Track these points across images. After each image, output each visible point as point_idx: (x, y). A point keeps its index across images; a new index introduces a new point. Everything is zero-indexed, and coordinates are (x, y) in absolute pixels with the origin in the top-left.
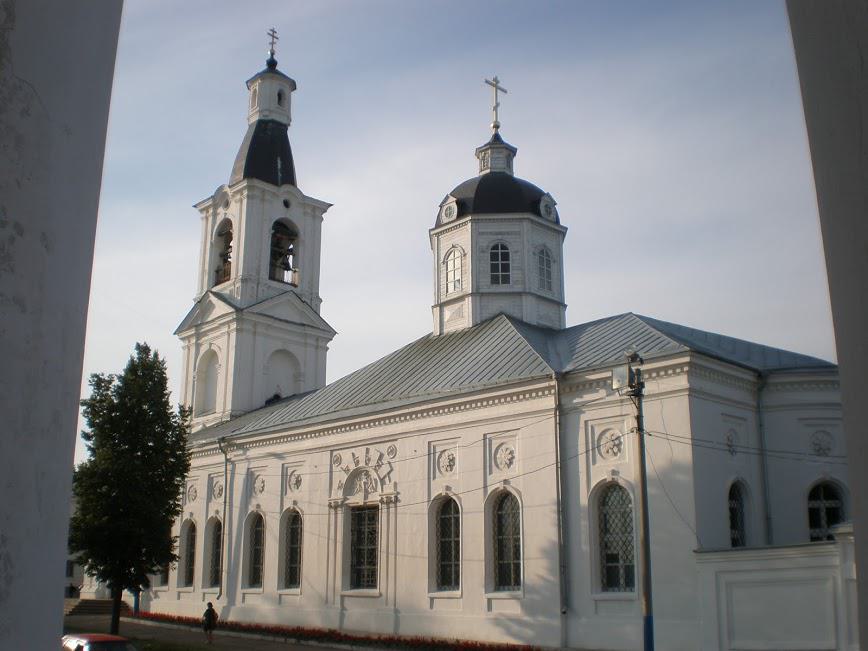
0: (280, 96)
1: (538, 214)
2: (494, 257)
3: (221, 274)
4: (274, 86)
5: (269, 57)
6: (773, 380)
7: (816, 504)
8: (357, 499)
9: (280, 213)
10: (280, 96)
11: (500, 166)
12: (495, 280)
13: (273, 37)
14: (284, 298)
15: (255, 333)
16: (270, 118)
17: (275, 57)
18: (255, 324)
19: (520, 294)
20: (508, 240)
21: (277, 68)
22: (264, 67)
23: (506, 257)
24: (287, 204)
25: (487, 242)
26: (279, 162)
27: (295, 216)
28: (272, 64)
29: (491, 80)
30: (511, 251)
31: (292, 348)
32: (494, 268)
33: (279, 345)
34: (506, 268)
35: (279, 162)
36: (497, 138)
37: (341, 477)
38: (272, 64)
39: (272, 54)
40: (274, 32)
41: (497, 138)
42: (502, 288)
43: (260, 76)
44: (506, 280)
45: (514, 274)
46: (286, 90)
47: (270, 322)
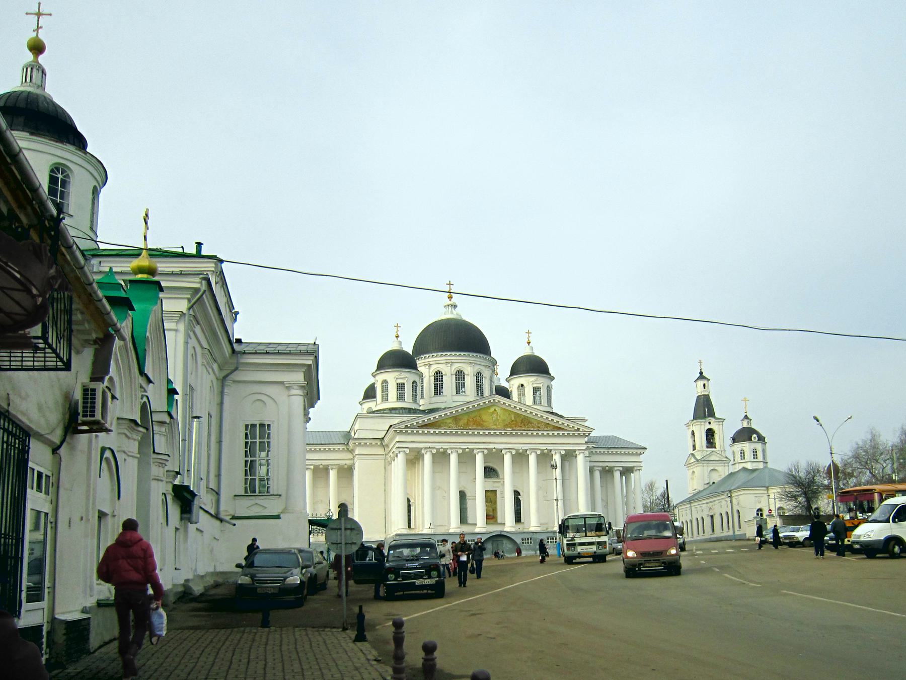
0: (704, 385)
1: (751, 440)
2: (741, 453)
3: (694, 447)
4: (701, 383)
5: (700, 371)
6: (769, 488)
7: (779, 511)
8: (712, 514)
9: (708, 426)
11: (745, 424)
12: (741, 459)
13: (700, 363)
14: (714, 453)
15: (703, 466)
16: (703, 394)
19: (746, 462)
20: (744, 448)
21: (703, 374)
22: (699, 375)
23: (744, 453)
24: (710, 423)
25: (739, 449)
26: (706, 409)
27: (712, 426)
28: (701, 373)
29: (743, 399)
30: (745, 451)
31: (716, 468)
32: (741, 456)
33: (712, 468)
34: (744, 455)
35: (706, 409)
37: (708, 509)
38: (701, 373)
39: (701, 370)
40: (700, 361)
42: (744, 461)
43: (698, 379)
44: (744, 459)
45: (746, 457)
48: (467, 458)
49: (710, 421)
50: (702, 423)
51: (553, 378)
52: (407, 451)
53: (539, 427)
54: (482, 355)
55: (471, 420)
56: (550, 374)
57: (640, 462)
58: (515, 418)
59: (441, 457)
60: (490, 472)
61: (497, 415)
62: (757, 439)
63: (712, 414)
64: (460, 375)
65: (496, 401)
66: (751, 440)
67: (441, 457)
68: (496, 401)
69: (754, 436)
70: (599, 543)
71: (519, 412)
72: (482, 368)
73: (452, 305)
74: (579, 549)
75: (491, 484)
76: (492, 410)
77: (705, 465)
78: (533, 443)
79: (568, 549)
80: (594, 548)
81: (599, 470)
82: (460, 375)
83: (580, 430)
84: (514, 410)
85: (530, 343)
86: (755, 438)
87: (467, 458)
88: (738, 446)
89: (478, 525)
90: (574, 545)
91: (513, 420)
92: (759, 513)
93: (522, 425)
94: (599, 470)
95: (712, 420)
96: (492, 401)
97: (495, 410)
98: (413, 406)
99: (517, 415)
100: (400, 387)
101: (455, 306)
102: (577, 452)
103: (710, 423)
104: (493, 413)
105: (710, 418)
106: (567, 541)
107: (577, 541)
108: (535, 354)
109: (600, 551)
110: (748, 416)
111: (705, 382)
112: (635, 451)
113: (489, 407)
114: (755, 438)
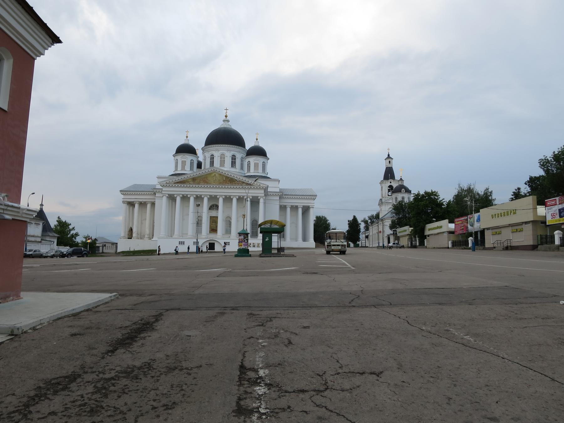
0: (390, 162)
1: (401, 192)
2: (396, 199)
4: (388, 161)
9: (389, 184)
10: (390, 162)
11: (400, 183)
17: (389, 154)
18: (385, 204)
23: (397, 199)
24: (391, 182)
25: (395, 197)
28: (389, 155)
30: (398, 197)
32: (396, 201)
36: (401, 178)
38: (389, 155)
41: (401, 178)
46: (391, 160)
47: (388, 203)
48: (199, 198)
49: (392, 182)
50: (386, 182)
51: (268, 159)
52: (167, 195)
53: (239, 184)
54: (241, 148)
55: (201, 180)
56: (267, 157)
57: (314, 203)
58: (225, 179)
59: (185, 198)
60: (214, 207)
61: (216, 177)
62: (404, 191)
63: (393, 177)
64: (222, 157)
65: (215, 170)
66: (401, 192)
67: (185, 198)
68: (215, 170)
69: (403, 189)
70: (342, 245)
71: (228, 176)
72: (236, 153)
73: (226, 120)
74: (333, 247)
75: (213, 213)
76: (213, 175)
77: (386, 205)
78: (235, 192)
79: (327, 248)
80: (340, 247)
81: (289, 207)
82: (222, 157)
83: (261, 186)
84: (225, 175)
85: (188, 137)
86: (403, 191)
87: (199, 198)
88: (395, 195)
89: (188, 234)
90: (330, 245)
91: (224, 180)
92: (395, 232)
93: (229, 183)
94: (289, 207)
95: (392, 180)
96: (213, 170)
97: (215, 175)
98: (263, 175)
99: (227, 177)
100: (184, 163)
101: (228, 121)
102: (259, 198)
103: (391, 182)
104: (213, 176)
105: (391, 180)
106: (327, 243)
107: (332, 244)
108: (260, 146)
109: (343, 249)
110: (402, 179)
111: (391, 160)
112: (312, 197)
113: (212, 173)
114: (403, 191)
